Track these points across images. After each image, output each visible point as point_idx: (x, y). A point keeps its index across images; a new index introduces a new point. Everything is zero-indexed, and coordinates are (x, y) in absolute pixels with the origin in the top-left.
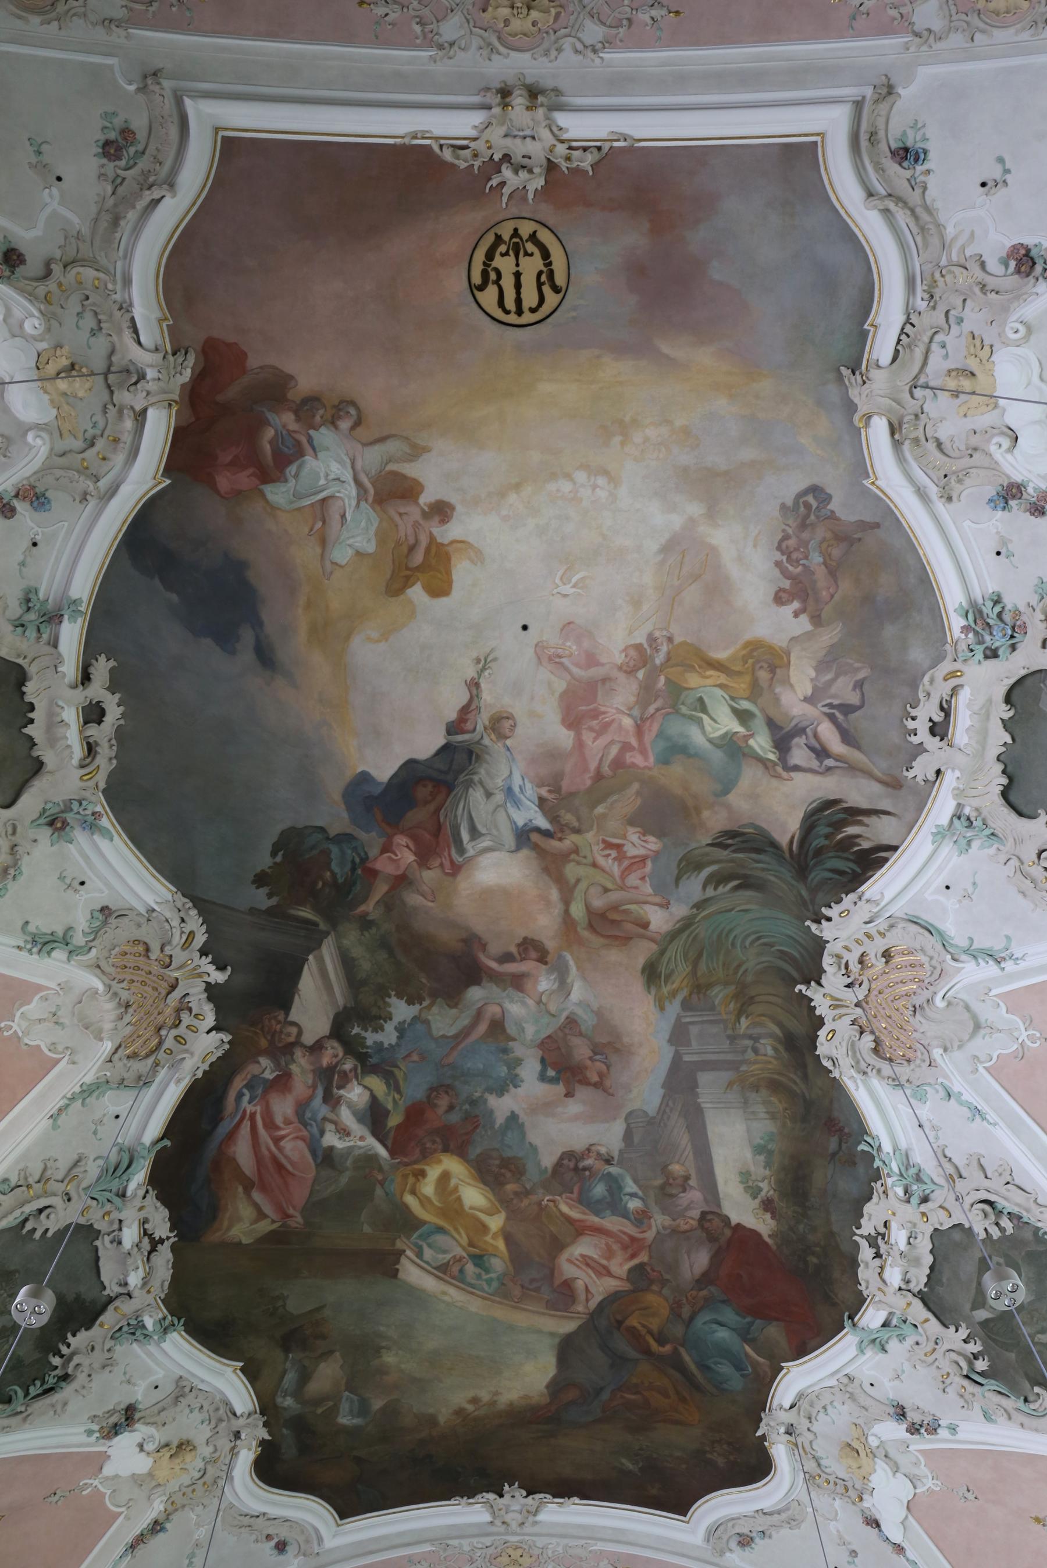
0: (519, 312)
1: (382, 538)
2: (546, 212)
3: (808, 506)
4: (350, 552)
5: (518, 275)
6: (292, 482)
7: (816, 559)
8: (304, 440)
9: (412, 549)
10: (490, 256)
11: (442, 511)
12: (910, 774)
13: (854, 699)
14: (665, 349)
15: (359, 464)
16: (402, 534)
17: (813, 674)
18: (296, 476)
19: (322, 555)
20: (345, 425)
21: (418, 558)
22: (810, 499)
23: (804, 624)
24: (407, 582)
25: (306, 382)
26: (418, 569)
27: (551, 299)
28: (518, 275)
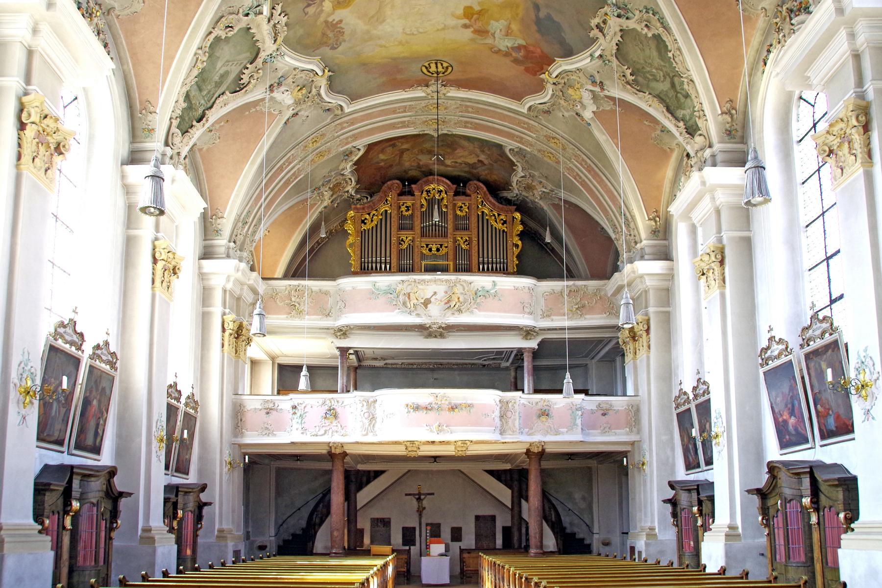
0: (436, 64)
1: (488, 23)
2: (427, 78)
3: (336, 44)
4: (500, 22)
5: (437, 67)
6: (516, 43)
7: (331, 35)
8: (510, 50)
9: (478, 19)
10: (446, 71)
11: (466, 26)
12: (281, 5)
13: (306, 10)
14: (389, 60)
15: (493, 40)
16: (480, 23)
17: (324, 8)
18: (515, 44)
19: (510, 24)
20: (495, 49)
21: (475, 16)
22: (336, 46)
23: (330, 19)
24: (480, 11)
25: (507, 61)
26: (475, 14)
27: (426, 64)
28: (437, 67)
